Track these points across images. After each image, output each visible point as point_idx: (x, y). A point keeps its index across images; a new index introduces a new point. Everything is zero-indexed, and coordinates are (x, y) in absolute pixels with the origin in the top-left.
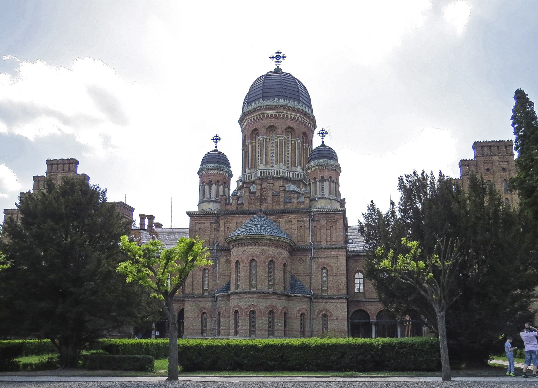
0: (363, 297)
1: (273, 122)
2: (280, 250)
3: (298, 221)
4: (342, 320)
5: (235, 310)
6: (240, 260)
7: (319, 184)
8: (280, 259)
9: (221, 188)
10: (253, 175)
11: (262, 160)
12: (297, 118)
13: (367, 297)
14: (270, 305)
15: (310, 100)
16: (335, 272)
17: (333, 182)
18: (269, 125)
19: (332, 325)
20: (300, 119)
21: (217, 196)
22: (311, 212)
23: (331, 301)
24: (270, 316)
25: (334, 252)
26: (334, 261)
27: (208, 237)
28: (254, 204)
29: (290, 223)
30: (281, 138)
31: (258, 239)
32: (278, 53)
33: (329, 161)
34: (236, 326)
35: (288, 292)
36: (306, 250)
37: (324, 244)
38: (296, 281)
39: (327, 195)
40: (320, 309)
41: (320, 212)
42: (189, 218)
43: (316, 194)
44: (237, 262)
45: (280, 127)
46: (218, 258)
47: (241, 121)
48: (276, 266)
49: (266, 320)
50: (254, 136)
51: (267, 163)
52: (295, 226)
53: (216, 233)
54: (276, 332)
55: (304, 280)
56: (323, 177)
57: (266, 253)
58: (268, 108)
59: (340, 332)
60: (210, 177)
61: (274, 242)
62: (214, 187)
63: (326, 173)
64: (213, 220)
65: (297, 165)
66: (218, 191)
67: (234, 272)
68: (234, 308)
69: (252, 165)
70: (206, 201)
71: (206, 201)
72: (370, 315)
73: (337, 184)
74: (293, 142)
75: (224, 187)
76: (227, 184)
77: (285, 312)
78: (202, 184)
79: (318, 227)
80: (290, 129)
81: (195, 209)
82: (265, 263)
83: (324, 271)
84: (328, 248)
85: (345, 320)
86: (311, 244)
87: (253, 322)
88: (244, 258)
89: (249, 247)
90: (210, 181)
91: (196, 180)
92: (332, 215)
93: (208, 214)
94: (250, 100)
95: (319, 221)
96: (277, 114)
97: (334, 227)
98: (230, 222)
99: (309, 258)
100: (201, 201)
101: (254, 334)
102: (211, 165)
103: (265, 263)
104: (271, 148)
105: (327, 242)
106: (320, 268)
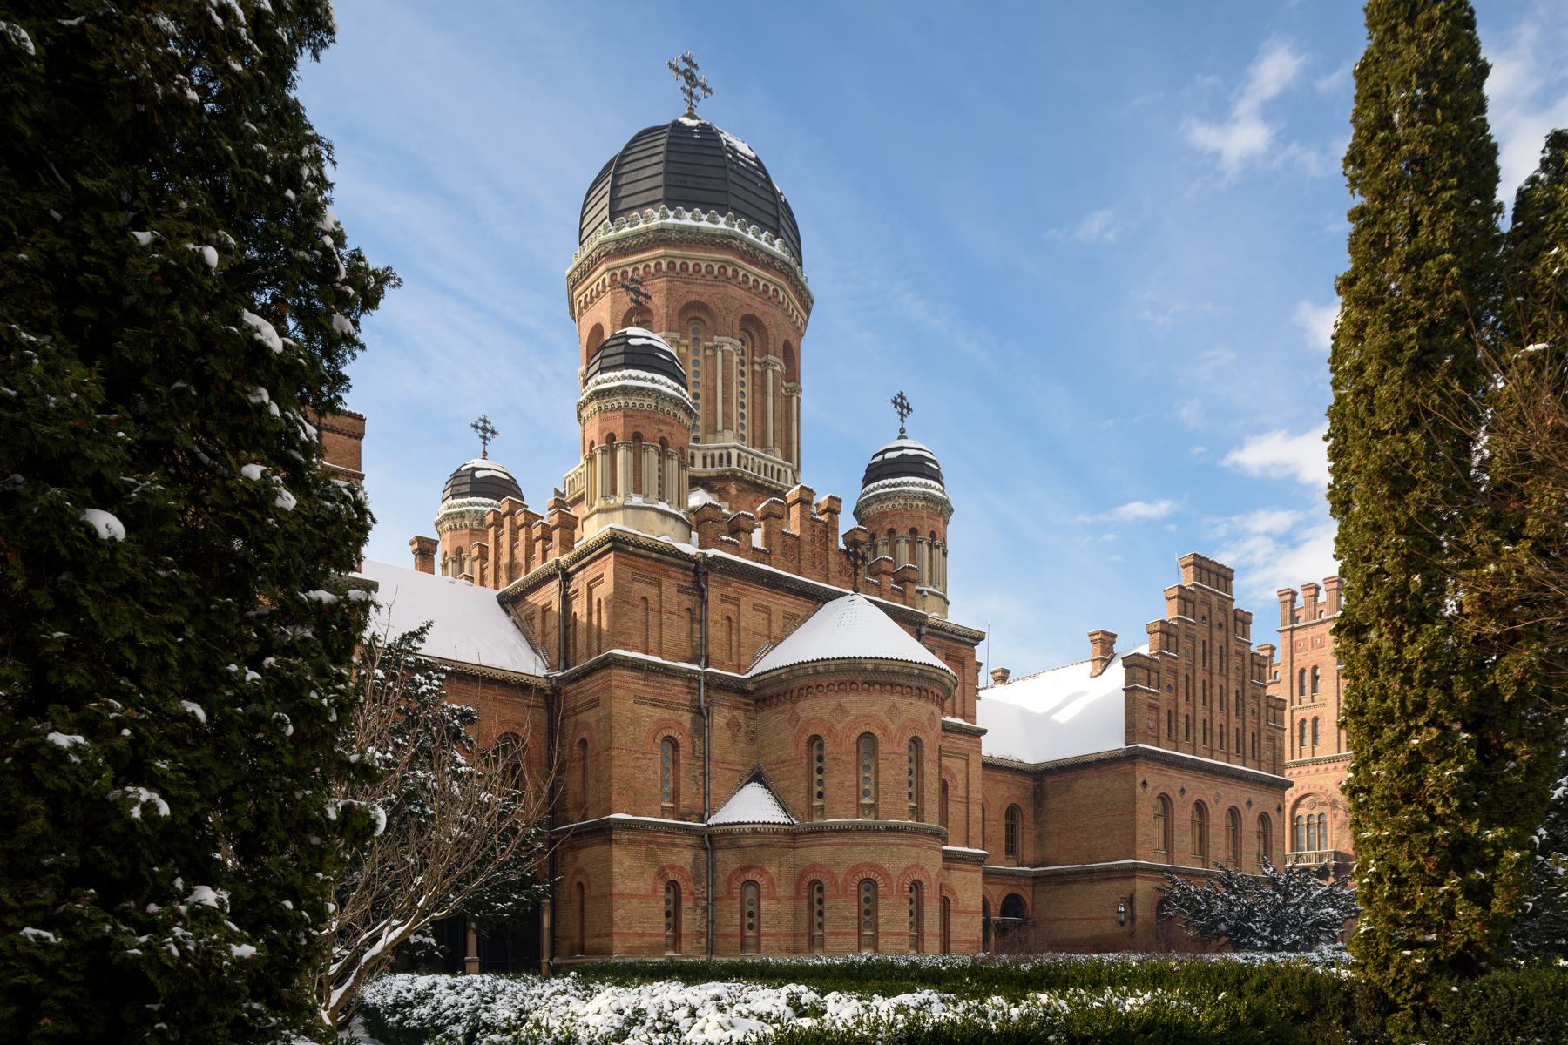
11: (727, 415)
30: (778, 368)
88: (893, 727)
89: (907, 701)
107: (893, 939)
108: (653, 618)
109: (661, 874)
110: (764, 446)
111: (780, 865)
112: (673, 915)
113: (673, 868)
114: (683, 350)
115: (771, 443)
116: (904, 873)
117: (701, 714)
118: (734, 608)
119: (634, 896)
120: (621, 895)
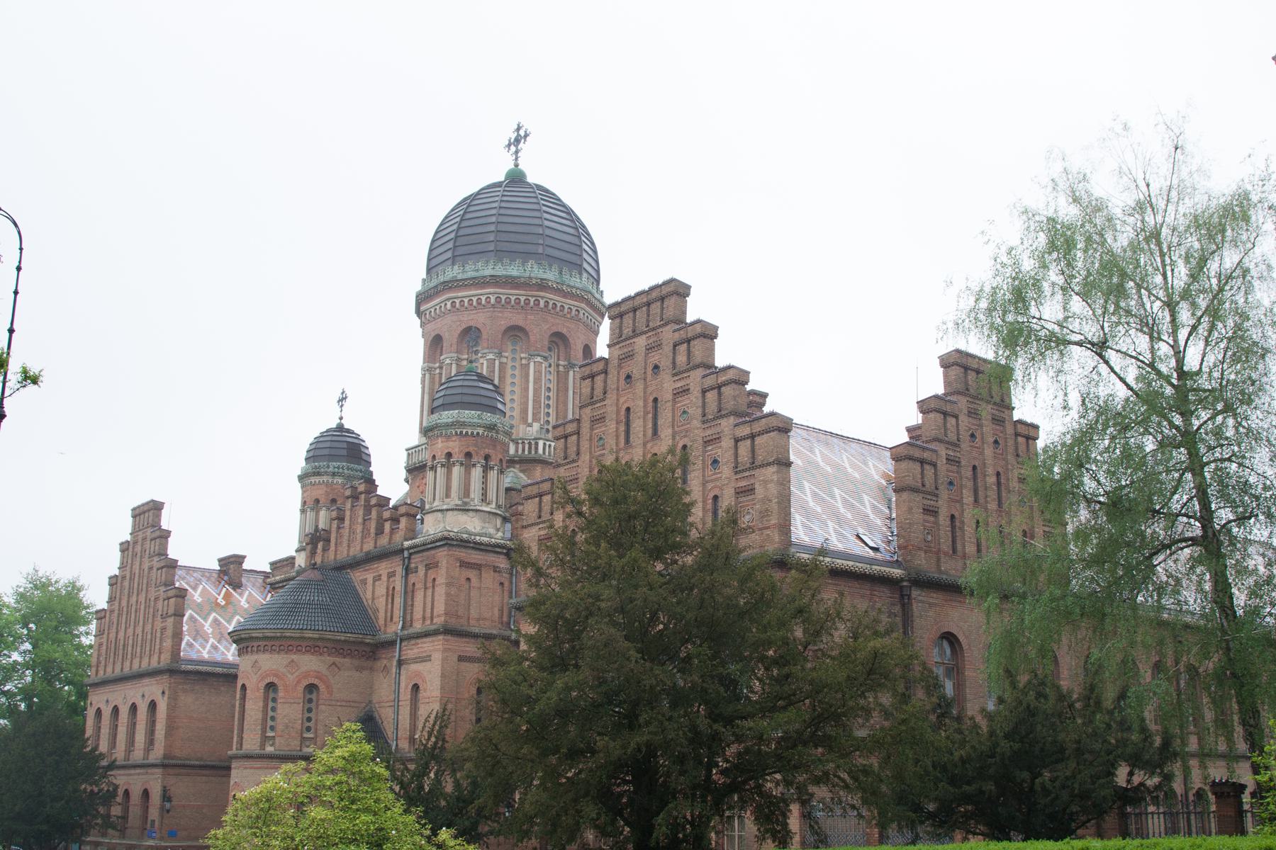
2: (294, 657)
8: (291, 678)
12: (483, 298)
16: (428, 694)
18: (433, 334)
20: (493, 301)
22: (402, 551)
25: (427, 645)
26: (428, 664)
30: (448, 361)
32: (519, 129)
36: (391, 643)
37: (418, 626)
48: (281, 694)
52: (381, 590)
56: (434, 457)
61: (277, 643)
82: (258, 690)
99: (395, 663)
105: (424, 619)
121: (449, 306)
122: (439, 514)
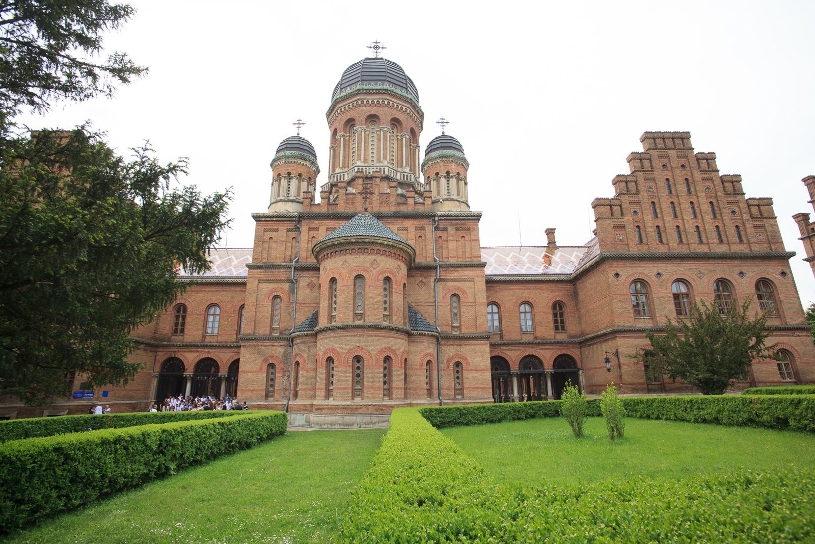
0: (499, 339)
1: (374, 110)
3: (416, 229)
4: (483, 370)
5: (327, 357)
6: (337, 276)
7: (443, 181)
9: (304, 185)
10: (346, 174)
13: (505, 338)
14: (385, 348)
15: (417, 94)
16: (471, 300)
17: (461, 180)
18: (369, 113)
19: (469, 379)
21: (299, 195)
22: (435, 216)
23: (467, 342)
24: (386, 365)
26: (470, 284)
27: (283, 249)
28: (352, 205)
29: (405, 232)
30: (386, 129)
31: (369, 243)
32: (377, 43)
33: (456, 153)
34: (329, 382)
35: (408, 328)
36: (429, 268)
37: (453, 261)
38: (416, 313)
39: (455, 196)
40: (451, 355)
41: (448, 217)
42: (255, 222)
43: (439, 193)
44: (333, 280)
45: (383, 116)
46: (296, 280)
47: (330, 113)
48: (394, 286)
49: (380, 371)
50: (348, 128)
51: (366, 160)
53: (295, 244)
54: (395, 391)
55: (426, 312)
56: (448, 173)
57: (379, 265)
58: (369, 92)
59: (481, 388)
60: (288, 168)
61: (392, 251)
62: (294, 182)
63: (453, 168)
64: (291, 225)
65: (404, 165)
66: (299, 188)
67: (327, 297)
68: (325, 352)
69: (344, 163)
70: (281, 201)
71: (281, 201)
72: (511, 363)
73: (466, 184)
74: (399, 137)
75: (309, 184)
76: (311, 181)
77: (406, 359)
78: (278, 178)
79: (444, 238)
80: (396, 122)
81: (264, 210)
82: (378, 280)
83: (455, 299)
84: (460, 266)
85: (487, 370)
86: (435, 260)
87: (358, 375)
88: (344, 272)
89: (354, 256)
90: (289, 174)
91: (269, 174)
92: (463, 222)
93: (285, 217)
94: (343, 86)
95: (445, 229)
96: (381, 101)
97: (467, 238)
98: (317, 229)
99: (433, 280)
100: (273, 200)
101: (359, 395)
102: (290, 152)
103: (378, 280)
104: (370, 143)
105: (458, 258)
106: (449, 295)
107: (341, 391)
108: (274, 245)
109: (265, 360)
110: (401, 166)
111: (309, 352)
112: (271, 381)
113: (272, 357)
114: (348, 138)
115: (404, 165)
116: (348, 352)
117: (293, 282)
118: (316, 232)
119: (251, 372)
120: (244, 372)
121: (386, 102)
122: (458, 203)
